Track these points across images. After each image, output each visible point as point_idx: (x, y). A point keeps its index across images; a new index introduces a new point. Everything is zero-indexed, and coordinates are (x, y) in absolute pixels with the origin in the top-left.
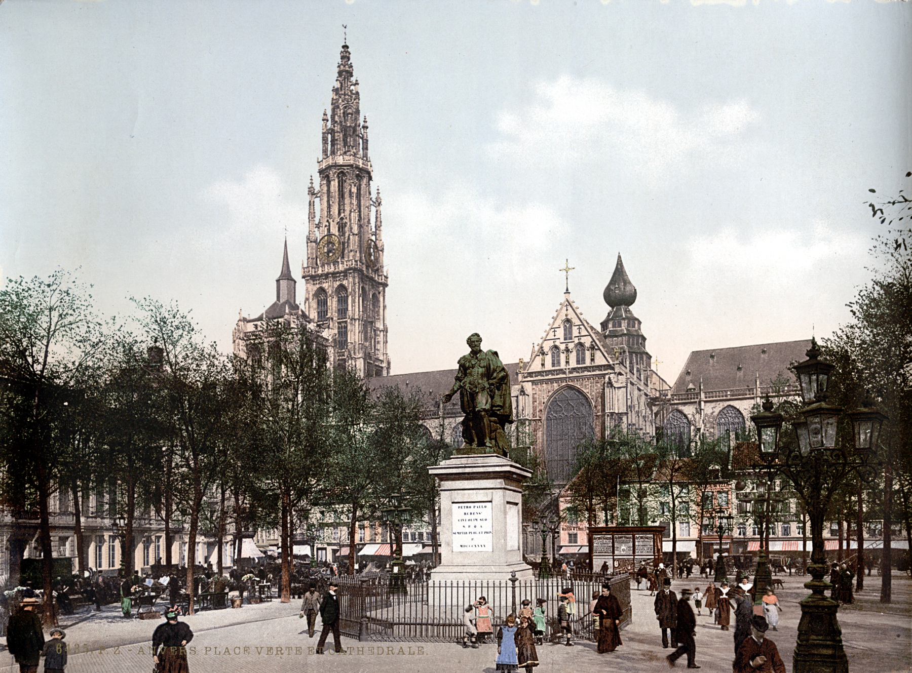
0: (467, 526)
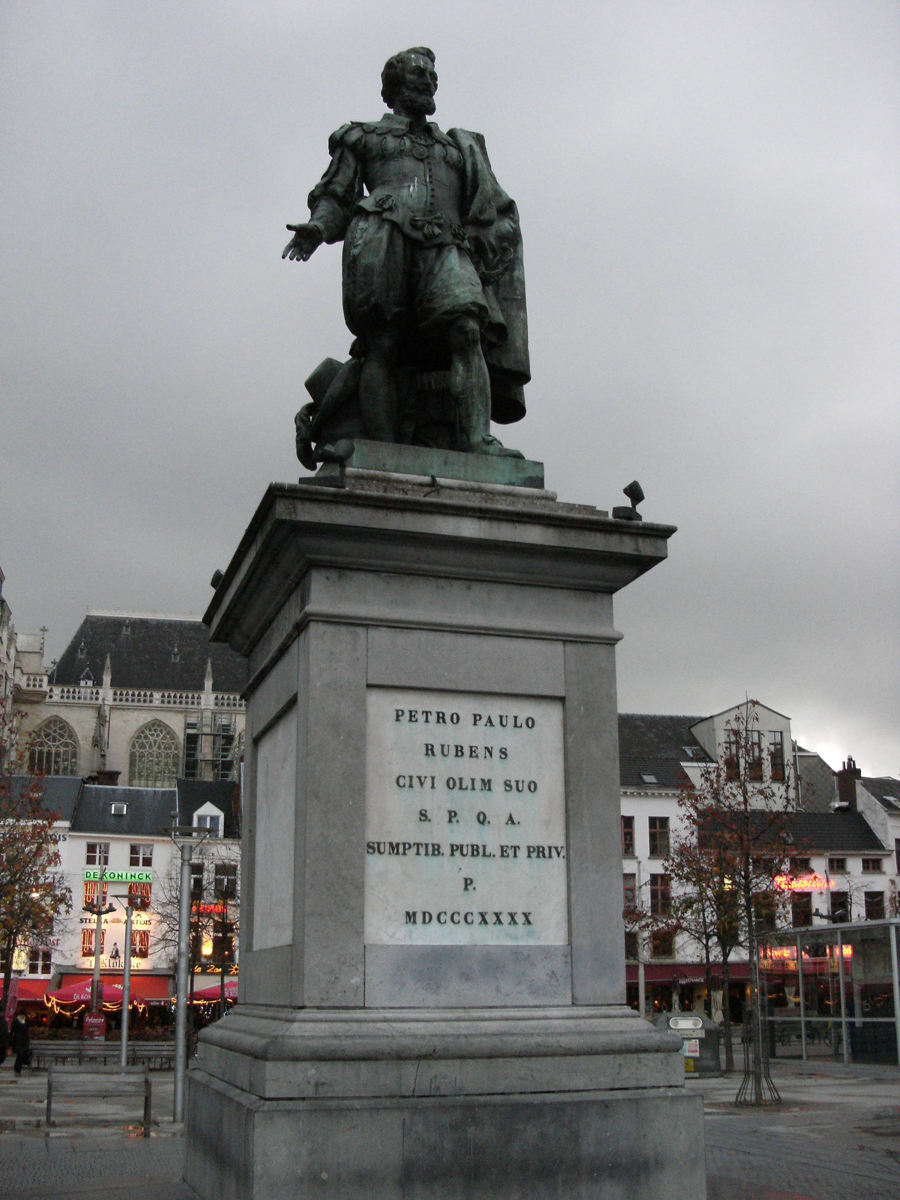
0: (439, 816)
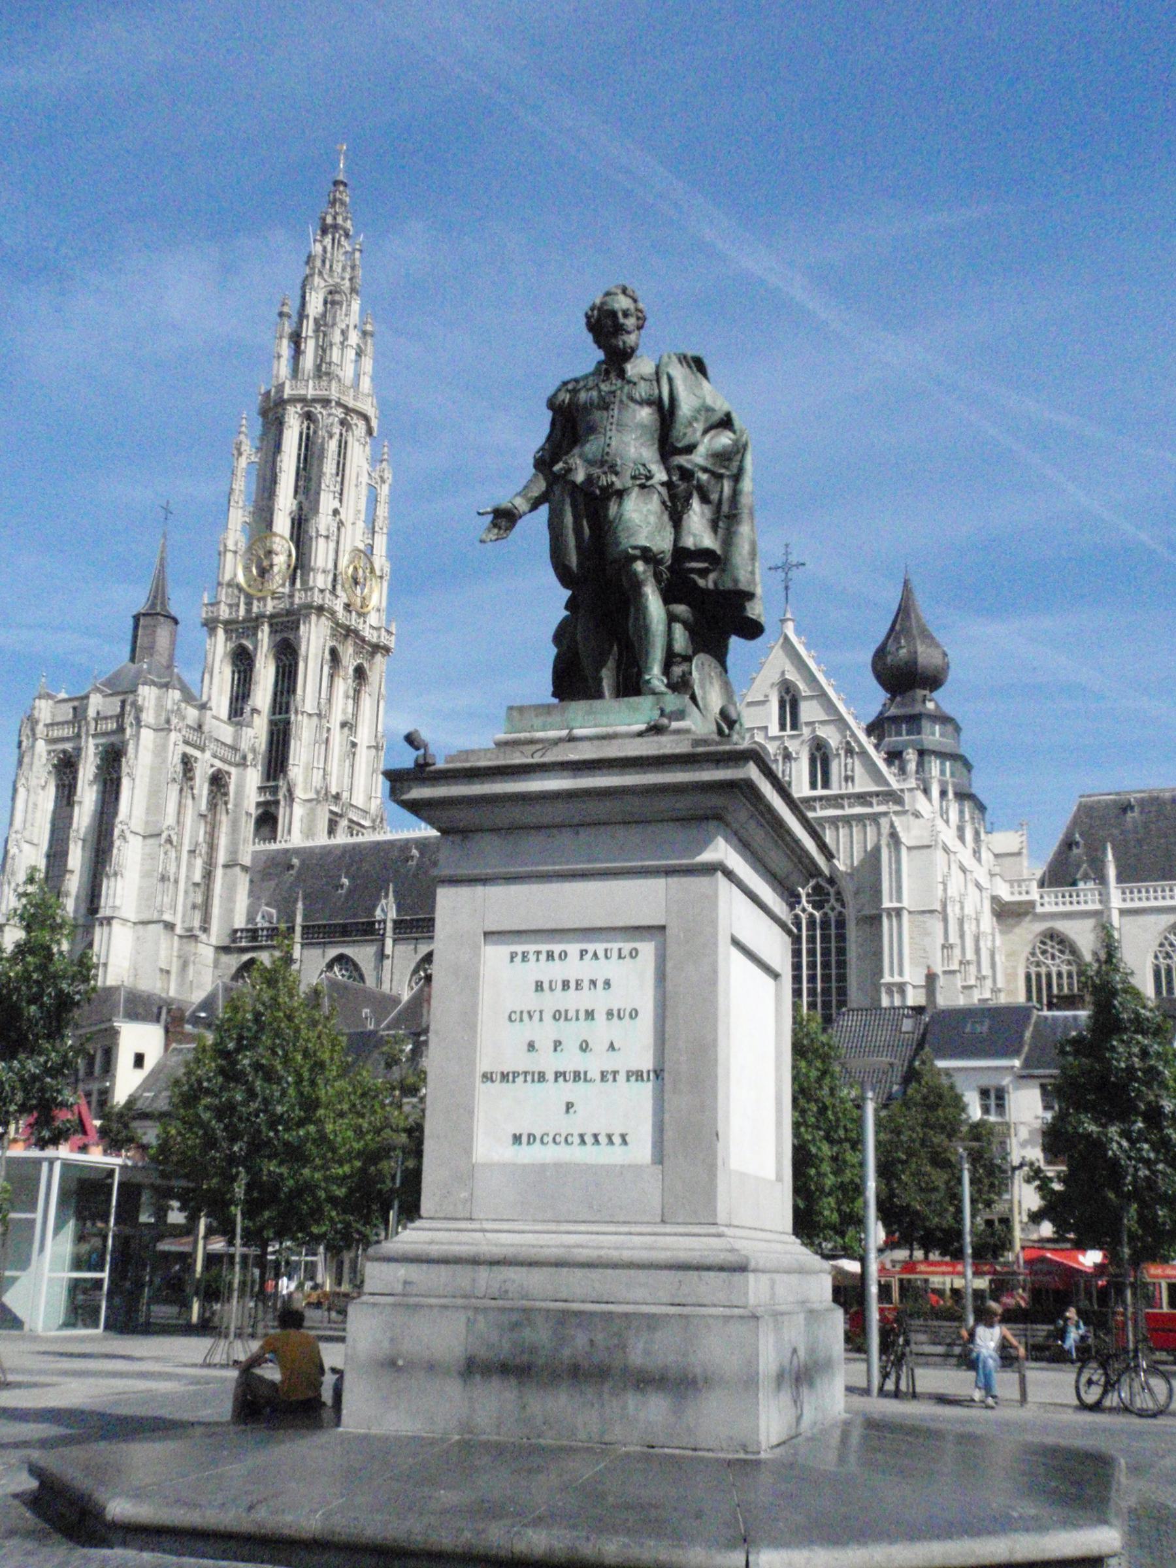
0: (545, 1045)
